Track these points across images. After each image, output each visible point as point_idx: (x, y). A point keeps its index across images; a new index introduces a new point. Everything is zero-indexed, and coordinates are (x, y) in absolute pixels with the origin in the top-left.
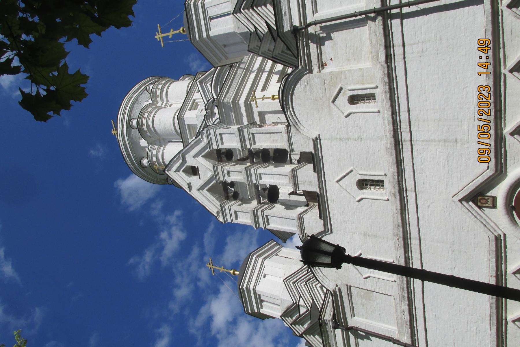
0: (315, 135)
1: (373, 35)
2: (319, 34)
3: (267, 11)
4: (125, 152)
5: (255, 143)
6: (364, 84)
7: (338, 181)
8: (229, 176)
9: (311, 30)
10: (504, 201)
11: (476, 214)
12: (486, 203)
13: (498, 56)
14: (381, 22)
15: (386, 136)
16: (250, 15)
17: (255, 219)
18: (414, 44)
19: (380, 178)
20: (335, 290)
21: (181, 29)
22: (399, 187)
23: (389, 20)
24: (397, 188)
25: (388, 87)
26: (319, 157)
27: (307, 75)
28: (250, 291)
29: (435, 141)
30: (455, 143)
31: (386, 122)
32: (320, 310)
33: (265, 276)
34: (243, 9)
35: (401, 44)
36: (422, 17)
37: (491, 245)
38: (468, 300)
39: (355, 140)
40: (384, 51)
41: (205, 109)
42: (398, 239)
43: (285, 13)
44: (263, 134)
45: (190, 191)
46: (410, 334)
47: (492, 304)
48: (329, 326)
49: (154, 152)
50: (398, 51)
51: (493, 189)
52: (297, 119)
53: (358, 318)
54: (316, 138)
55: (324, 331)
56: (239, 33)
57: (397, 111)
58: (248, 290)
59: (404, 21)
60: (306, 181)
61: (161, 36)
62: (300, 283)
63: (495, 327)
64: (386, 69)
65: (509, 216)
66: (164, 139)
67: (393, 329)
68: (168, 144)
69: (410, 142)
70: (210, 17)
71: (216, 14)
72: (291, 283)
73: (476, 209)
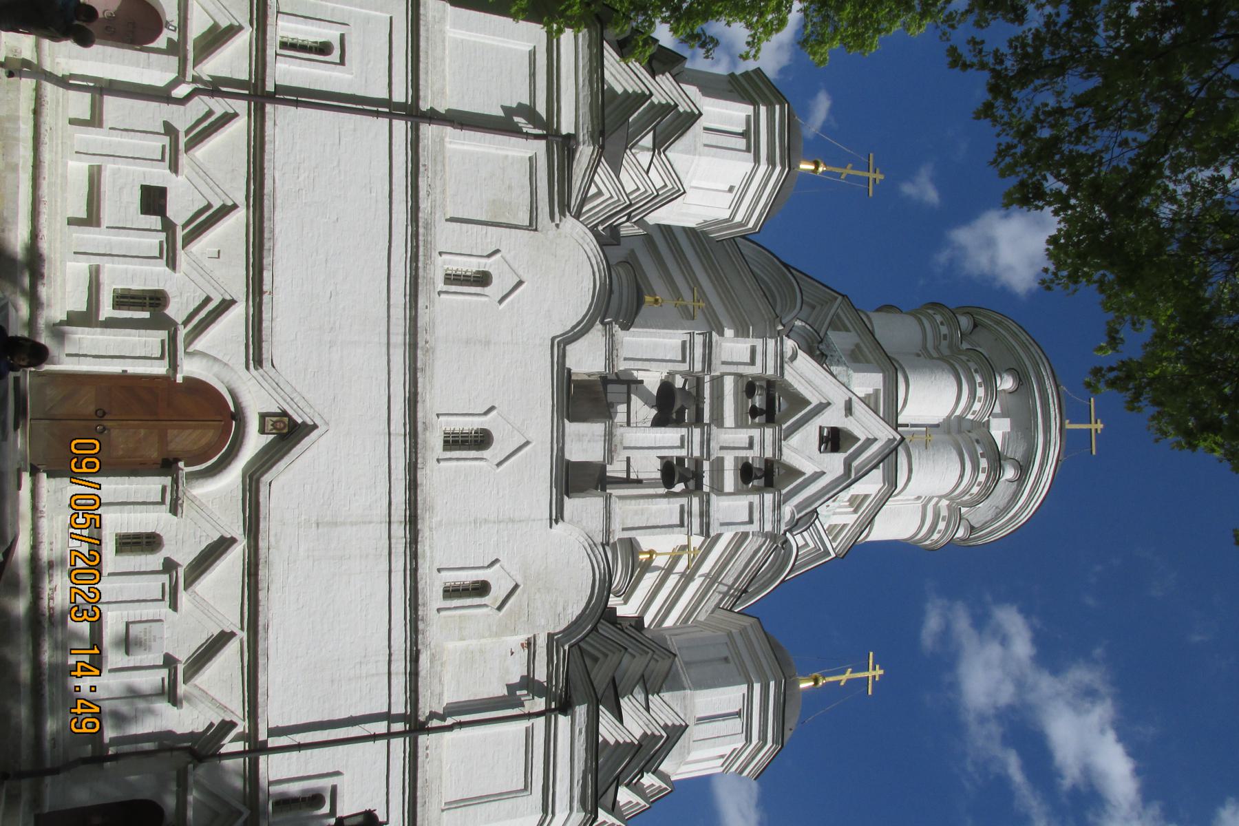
0: (559, 528)
1: (437, 691)
2: (528, 695)
3: (614, 733)
4: (1052, 409)
5: (682, 507)
6: (460, 616)
7: (527, 443)
8: (751, 439)
9: (540, 704)
10: (247, 430)
11: (291, 403)
12: (275, 422)
13: (251, 655)
14: (420, 713)
15: (431, 529)
16: (651, 726)
17: (710, 353)
18: (373, 675)
19: (449, 454)
20: (563, 217)
21: (821, 684)
22: (416, 443)
23: (409, 713)
24: (420, 441)
25: (420, 613)
26: (556, 488)
27: (557, 630)
28: (768, 159)
29: (352, 524)
30: (320, 521)
31: (428, 554)
32: (603, 159)
33: (731, 189)
34: (662, 737)
35: (393, 677)
36: (358, 714)
37: (268, 351)
38: (310, 235)
39: (486, 520)
40: (420, 669)
41: (818, 514)
42: (427, 342)
43: (580, 732)
44: (660, 524)
45: (850, 399)
46: (421, 145)
47: (270, 239)
48: (585, 131)
49: (977, 406)
50: (399, 666)
51: (264, 447)
53: (522, 154)
54: (557, 522)
55: (597, 117)
56: (684, 689)
57: (408, 572)
58: (771, 161)
59: (385, 709)
60: (589, 441)
61: (870, 674)
62: (647, 194)
63: (266, 191)
64: (419, 642)
65: (240, 403)
66: (949, 433)
67: (455, 143)
68: (941, 421)
69: (393, 519)
70: (740, 717)
71: (726, 721)
72: (670, 186)
73: (290, 412)
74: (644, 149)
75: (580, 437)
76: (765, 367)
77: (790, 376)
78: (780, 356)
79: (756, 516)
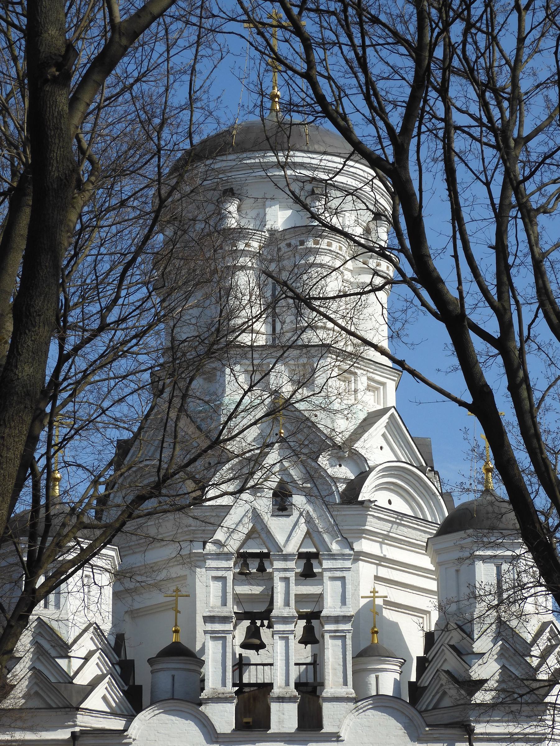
0: (344, 735)
5: (332, 637)
52: (364, 711)
74: (69, 666)
75: (280, 722)
76: (228, 569)
77: (233, 546)
78: (218, 556)
79: (338, 574)
